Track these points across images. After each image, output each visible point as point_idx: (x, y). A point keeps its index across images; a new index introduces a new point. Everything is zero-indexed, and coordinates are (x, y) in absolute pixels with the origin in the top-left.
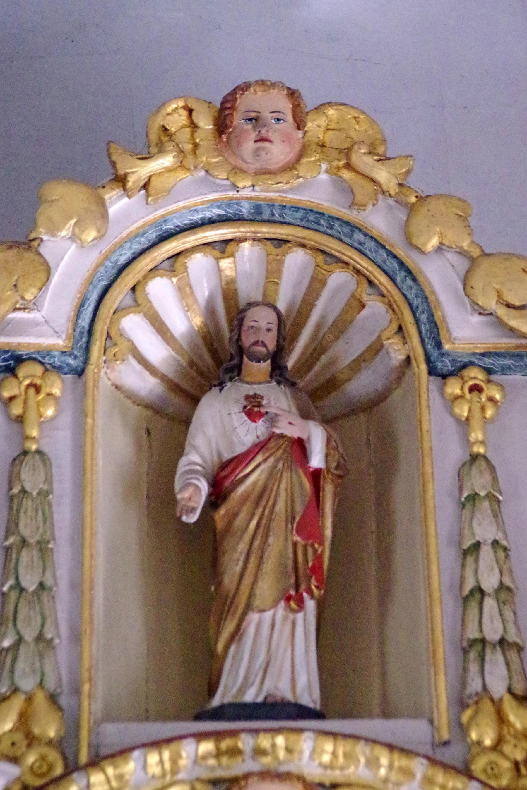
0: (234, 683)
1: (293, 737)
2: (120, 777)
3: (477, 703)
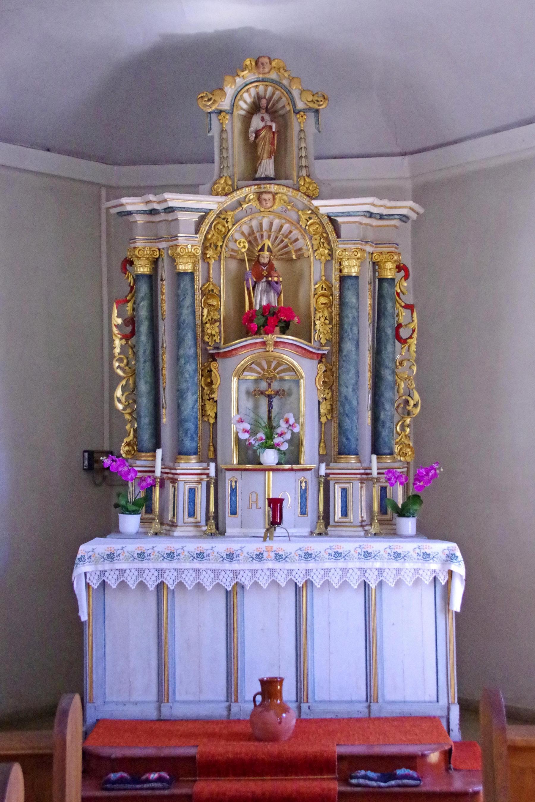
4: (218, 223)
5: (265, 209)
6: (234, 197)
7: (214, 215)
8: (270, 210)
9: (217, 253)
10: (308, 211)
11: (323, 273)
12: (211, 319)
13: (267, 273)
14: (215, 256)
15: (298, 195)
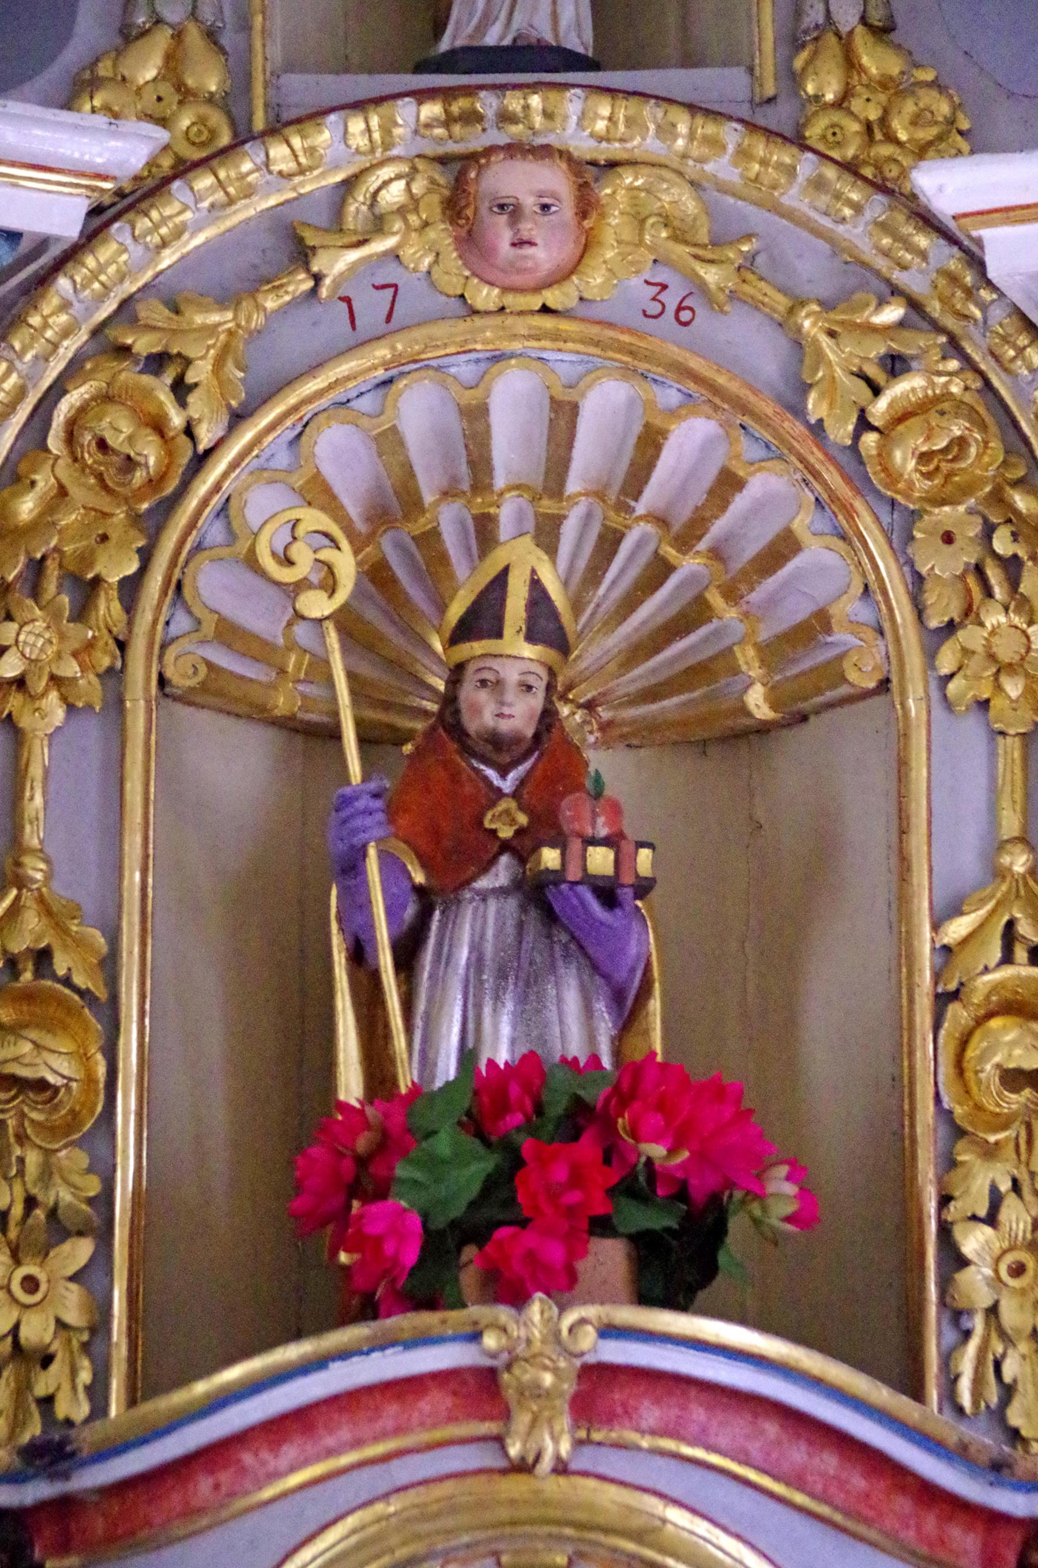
0: (471, 15)
1: (553, 95)
2: (311, 151)
3: (816, 39)
4: (106, 398)
5: (506, 289)
6: (249, 192)
7: (66, 333)
8: (552, 297)
9: (90, 645)
10: (882, 303)
11: (1011, 823)
12: (17, 1211)
13: (523, 819)
14: (71, 669)
15: (791, 172)
